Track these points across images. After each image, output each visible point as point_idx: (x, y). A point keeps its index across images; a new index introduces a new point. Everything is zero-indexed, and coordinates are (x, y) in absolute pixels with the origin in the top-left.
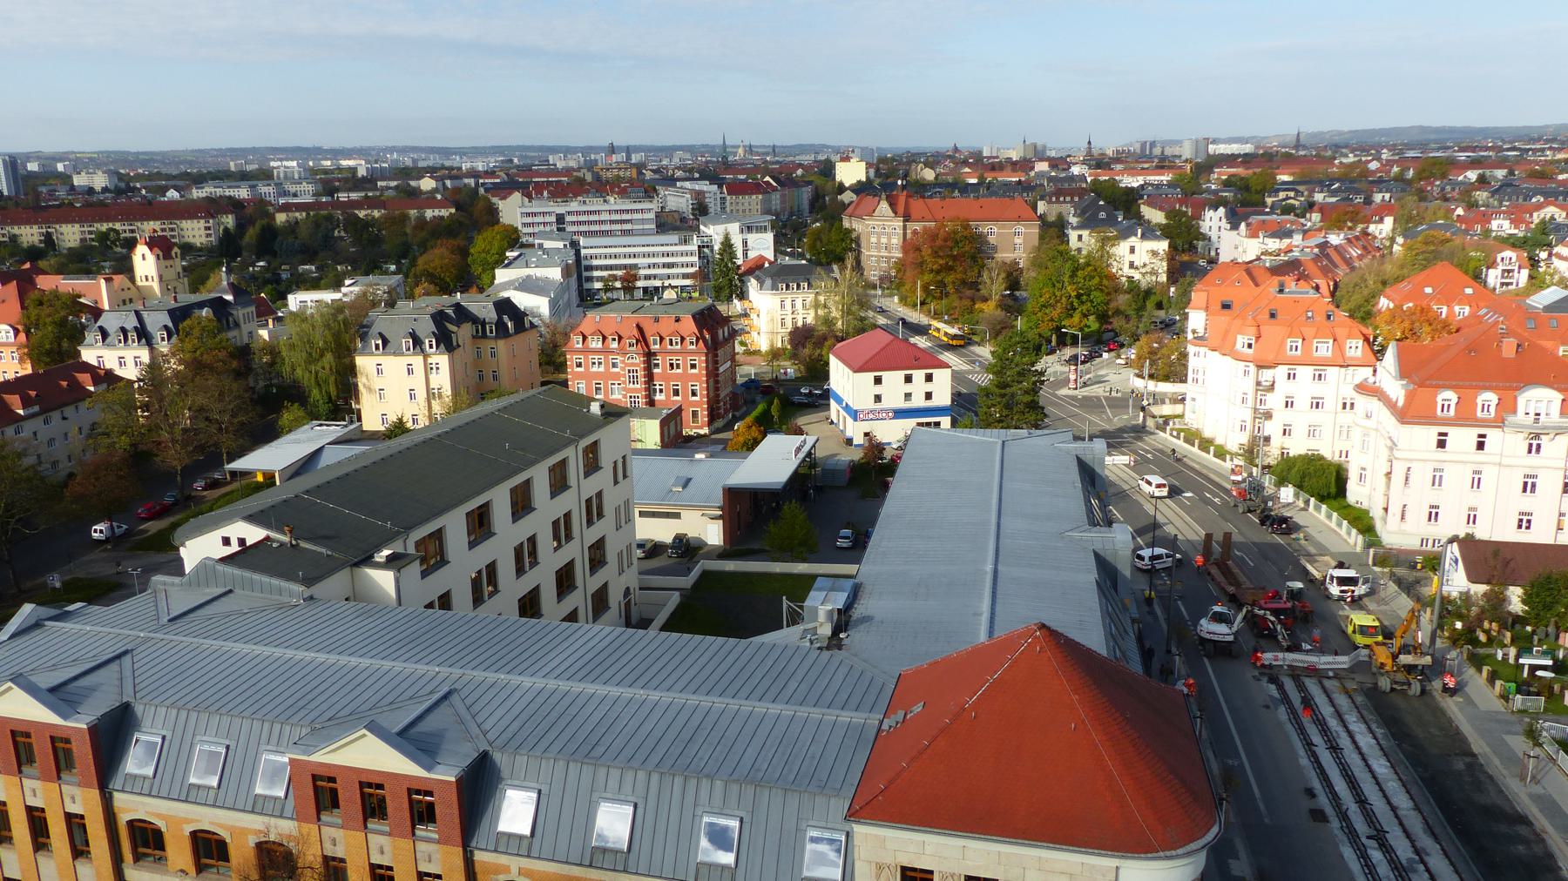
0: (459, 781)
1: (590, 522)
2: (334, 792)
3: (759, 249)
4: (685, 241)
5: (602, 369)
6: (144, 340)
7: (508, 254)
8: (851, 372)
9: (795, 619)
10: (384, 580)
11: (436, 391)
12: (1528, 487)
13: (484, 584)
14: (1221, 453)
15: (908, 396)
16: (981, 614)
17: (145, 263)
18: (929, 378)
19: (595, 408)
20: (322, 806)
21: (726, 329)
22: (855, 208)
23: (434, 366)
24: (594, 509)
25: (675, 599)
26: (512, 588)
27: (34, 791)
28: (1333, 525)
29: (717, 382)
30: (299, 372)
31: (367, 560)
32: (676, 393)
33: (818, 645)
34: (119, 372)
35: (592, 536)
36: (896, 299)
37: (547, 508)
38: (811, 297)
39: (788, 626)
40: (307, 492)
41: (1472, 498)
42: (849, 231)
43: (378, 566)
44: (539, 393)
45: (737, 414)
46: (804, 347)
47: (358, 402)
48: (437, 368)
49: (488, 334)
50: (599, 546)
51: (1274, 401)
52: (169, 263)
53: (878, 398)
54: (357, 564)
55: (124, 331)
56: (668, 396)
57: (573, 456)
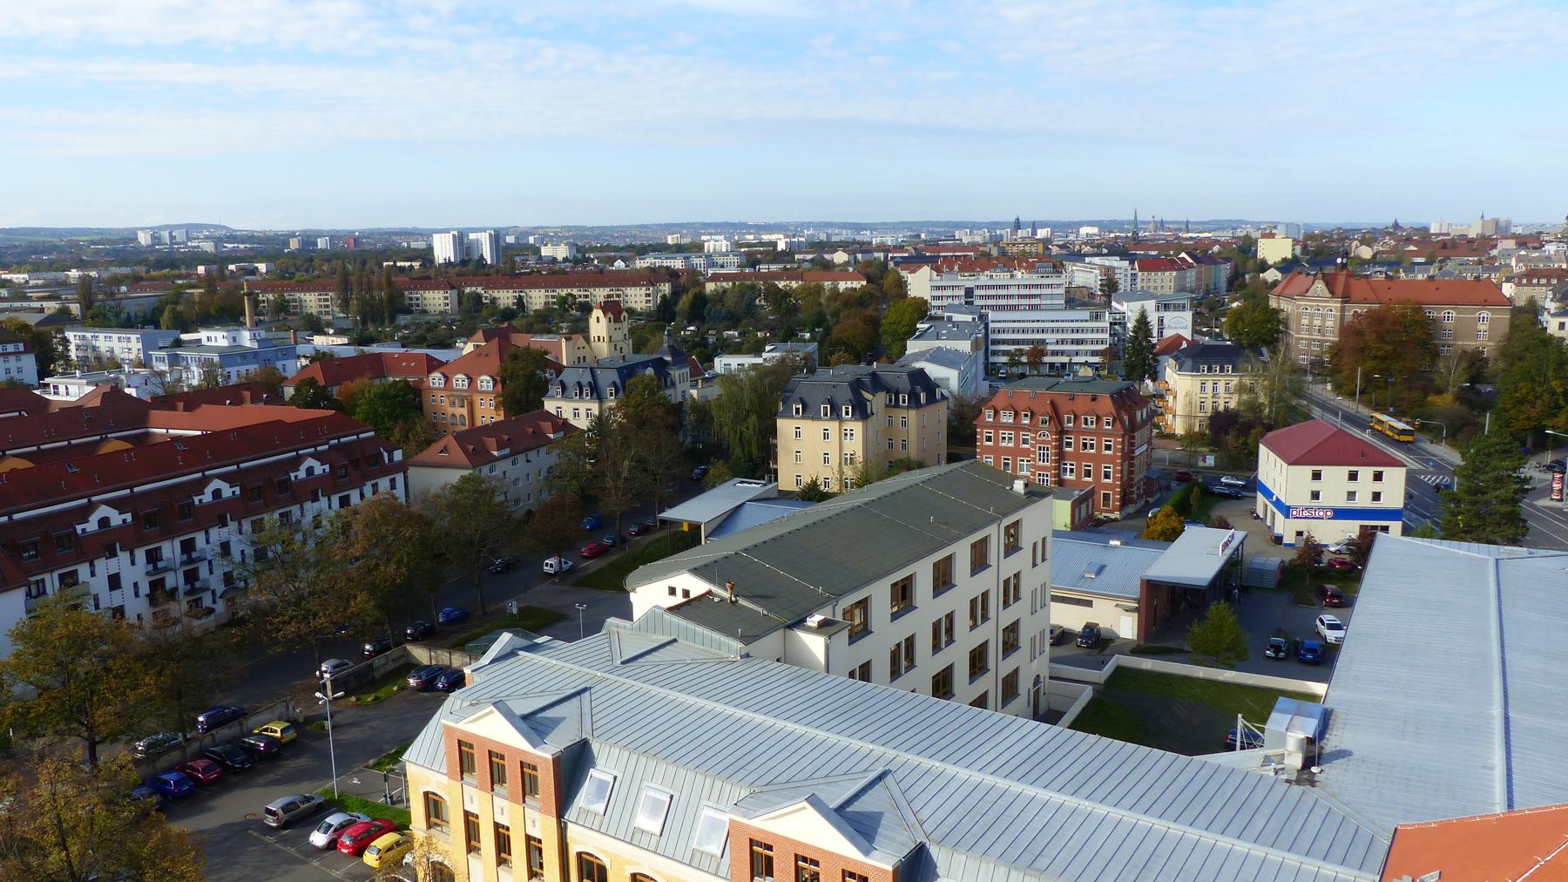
0: (896, 871)
1: (1006, 604)
2: (769, 860)
3: (1175, 328)
4: (1097, 318)
5: (1011, 445)
6: (595, 394)
7: (918, 326)
8: (1285, 465)
9: (1252, 741)
10: (815, 645)
11: (848, 456)
13: (902, 659)
15: (1351, 495)
16: (1492, 768)
17: (599, 325)
18: (1378, 477)
19: (1019, 486)
20: (755, 872)
21: (1145, 411)
22: (1284, 288)
23: (848, 432)
24: (1011, 591)
25: (1087, 693)
26: (928, 664)
27: (502, 810)
29: (1132, 465)
30: (725, 429)
31: (799, 623)
32: (1088, 474)
33: (1285, 777)
34: (573, 422)
35: (1007, 618)
36: (1329, 387)
37: (967, 585)
38: (1235, 381)
39: (1242, 748)
40: (746, 550)
42: (1276, 312)
43: (809, 630)
44: (962, 467)
45: (1151, 500)
46: (1227, 433)
47: (776, 462)
48: (852, 435)
49: (901, 403)
50: (1013, 629)
52: (618, 325)
53: (1315, 495)
54: (791, 627)
55: (580, 385)
56: (1079, 476)
57: (995, 534)
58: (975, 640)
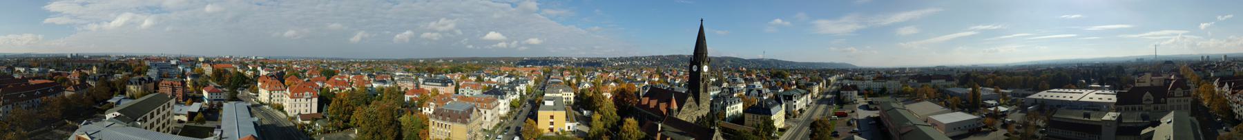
26: (156, 126)
41: (295, 108)
58: (163, 122)
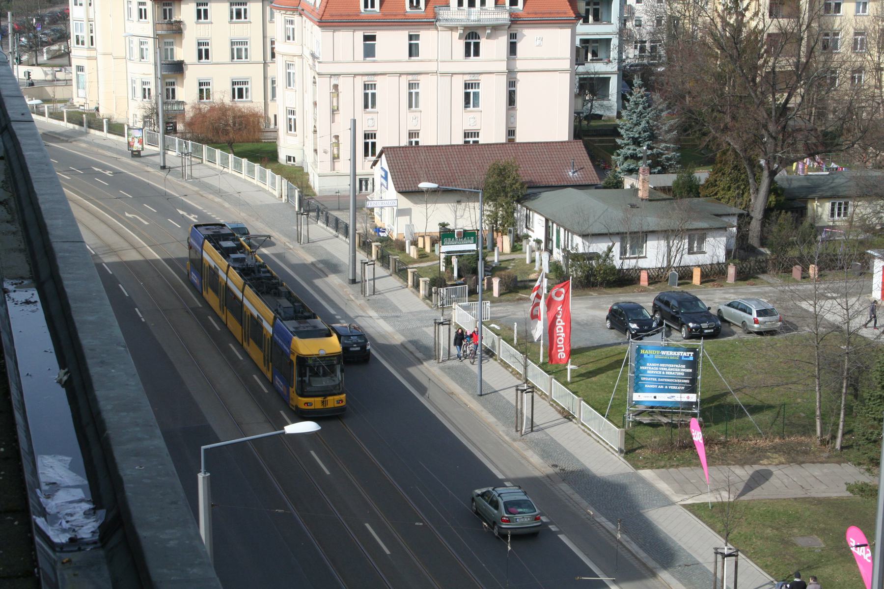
12: (469, 99)
14: (116, 129)
28: (256, 181)
51: (185, 52)
